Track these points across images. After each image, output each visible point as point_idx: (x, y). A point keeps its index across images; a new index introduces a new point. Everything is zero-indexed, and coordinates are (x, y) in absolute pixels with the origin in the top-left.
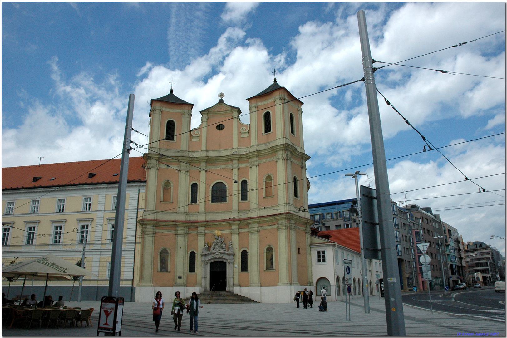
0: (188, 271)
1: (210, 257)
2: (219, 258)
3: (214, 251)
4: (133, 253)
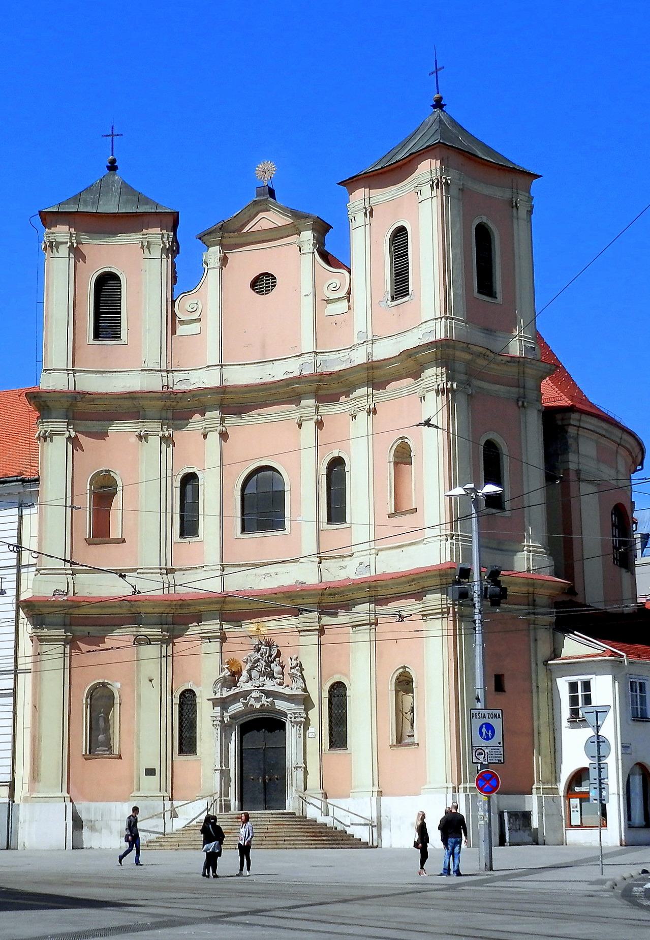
1: (236, 707)
2: (263, 709)
3: (248, 687)
4: (10, 700)
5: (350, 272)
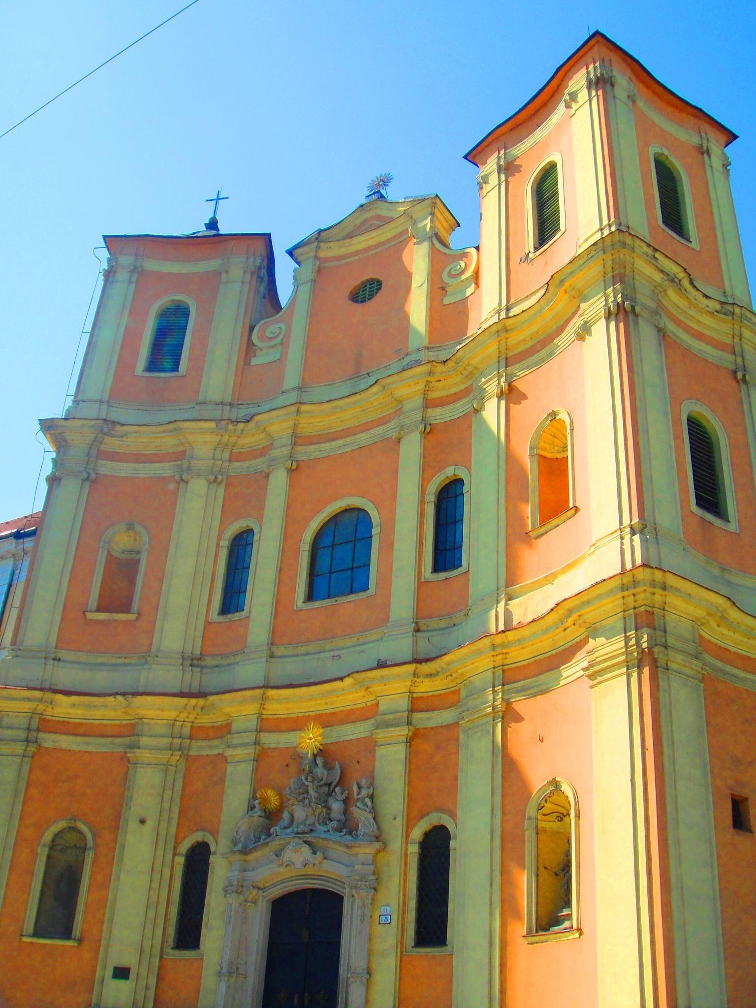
0: (171, 940)
5: (478, 248)
